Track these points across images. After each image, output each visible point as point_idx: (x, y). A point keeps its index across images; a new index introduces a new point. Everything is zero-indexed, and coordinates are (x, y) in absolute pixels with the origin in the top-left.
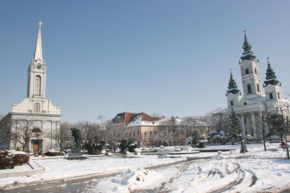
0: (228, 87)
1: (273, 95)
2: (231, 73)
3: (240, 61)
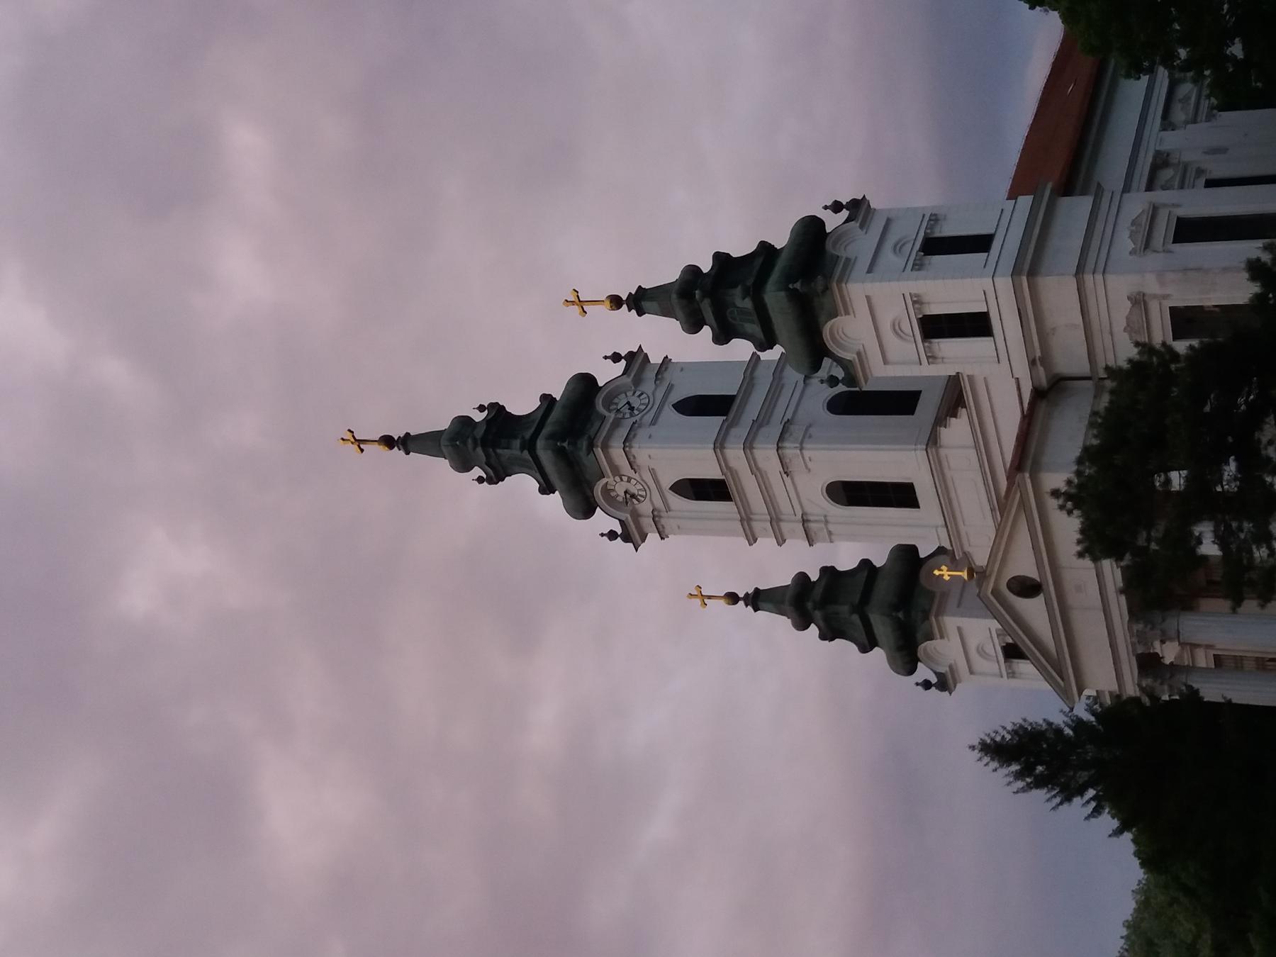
0: (864, 649)
3: (612, 535)
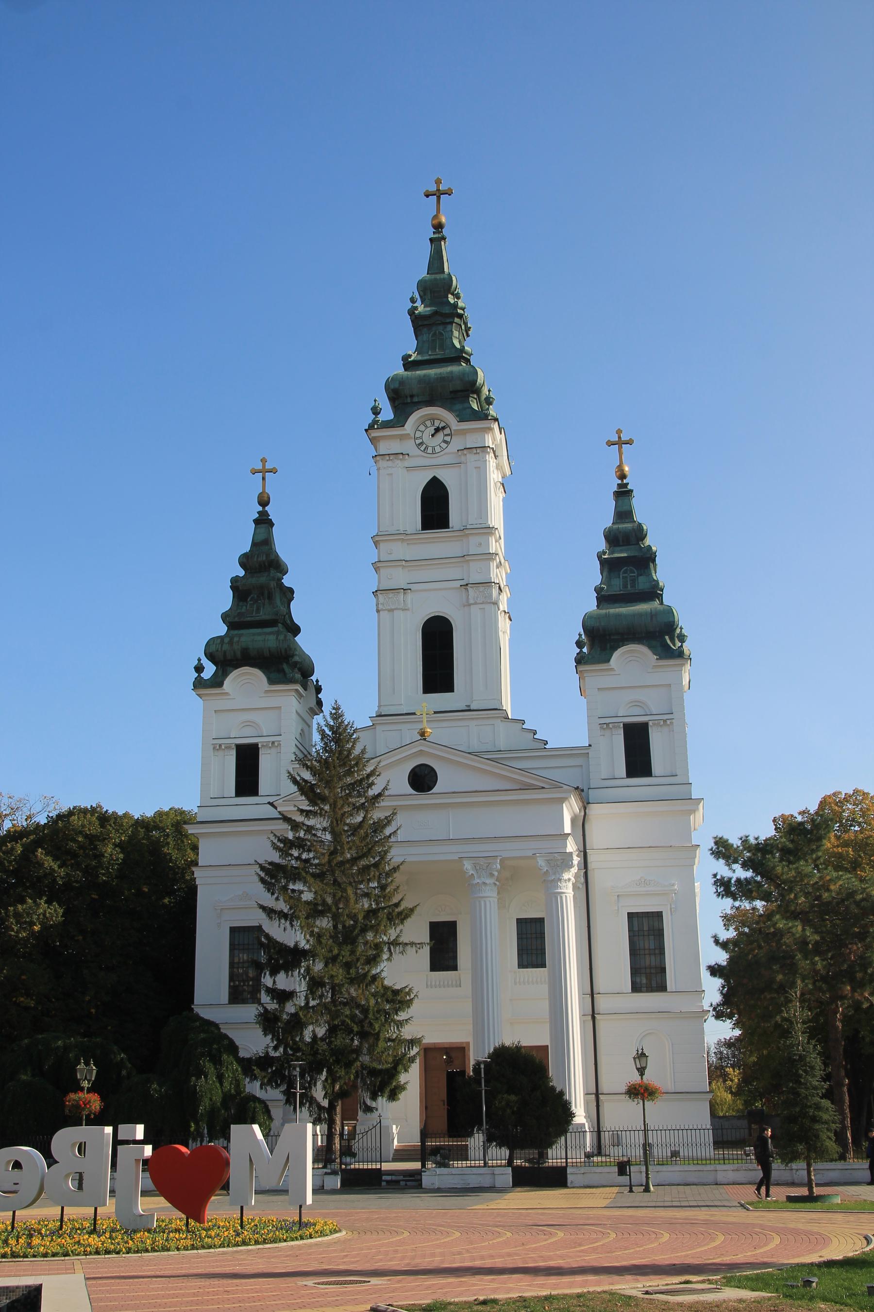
0: (225, 617)
1: (657, 741)
2: (264, 501)
